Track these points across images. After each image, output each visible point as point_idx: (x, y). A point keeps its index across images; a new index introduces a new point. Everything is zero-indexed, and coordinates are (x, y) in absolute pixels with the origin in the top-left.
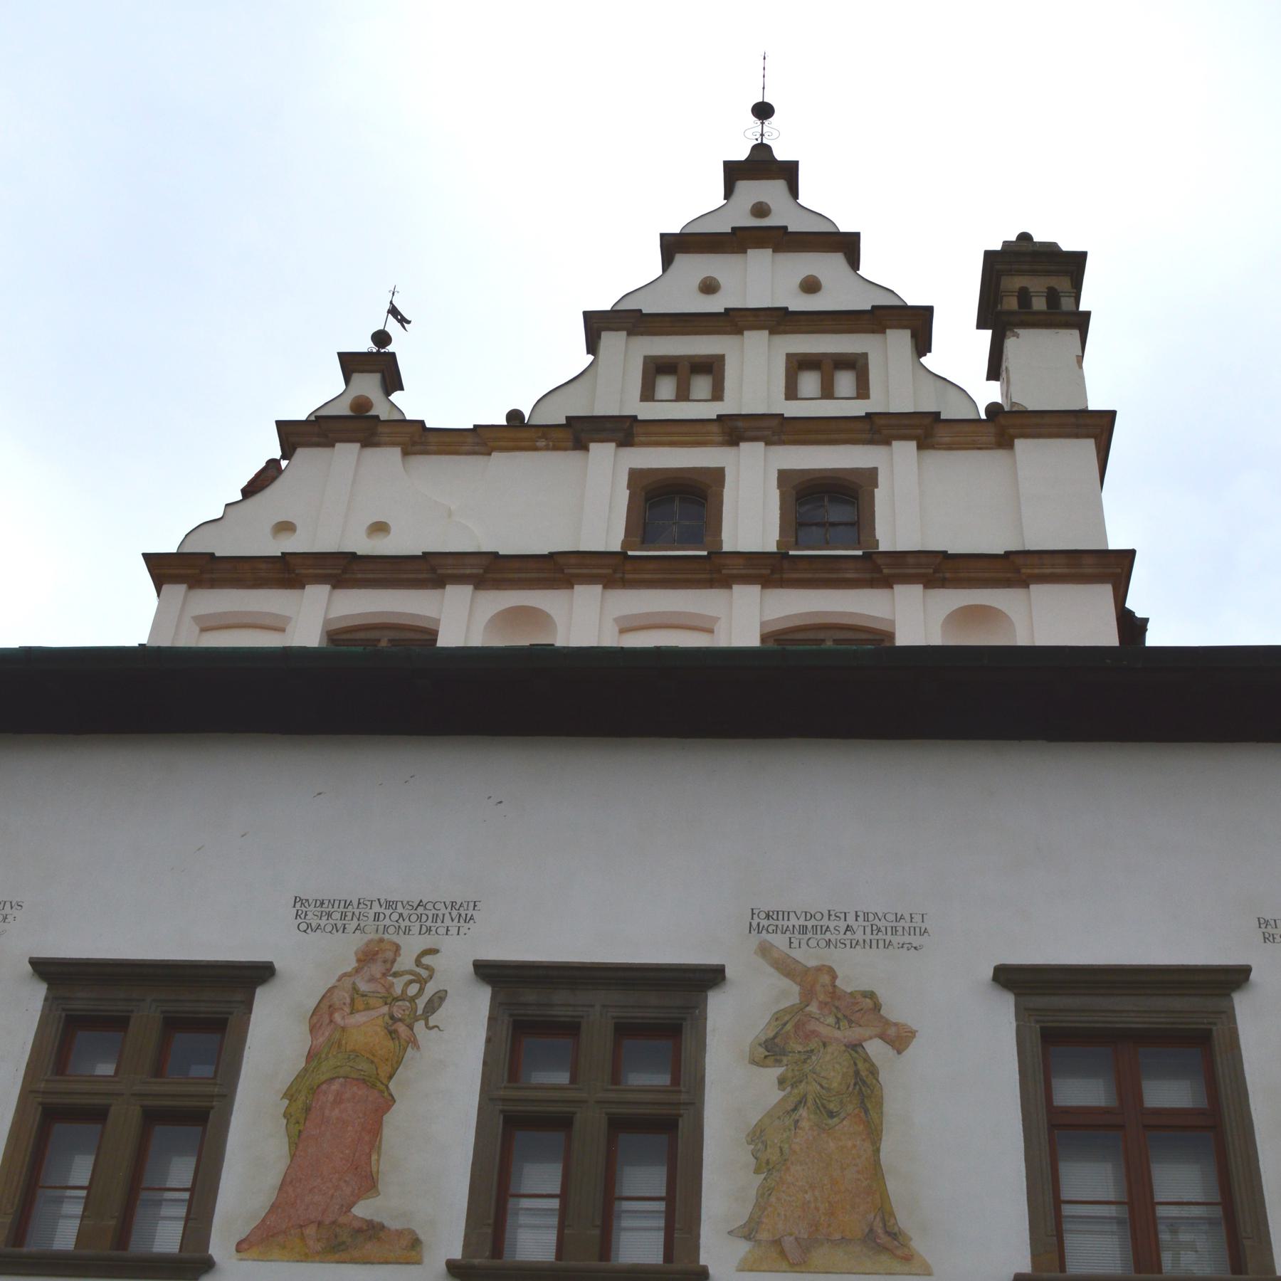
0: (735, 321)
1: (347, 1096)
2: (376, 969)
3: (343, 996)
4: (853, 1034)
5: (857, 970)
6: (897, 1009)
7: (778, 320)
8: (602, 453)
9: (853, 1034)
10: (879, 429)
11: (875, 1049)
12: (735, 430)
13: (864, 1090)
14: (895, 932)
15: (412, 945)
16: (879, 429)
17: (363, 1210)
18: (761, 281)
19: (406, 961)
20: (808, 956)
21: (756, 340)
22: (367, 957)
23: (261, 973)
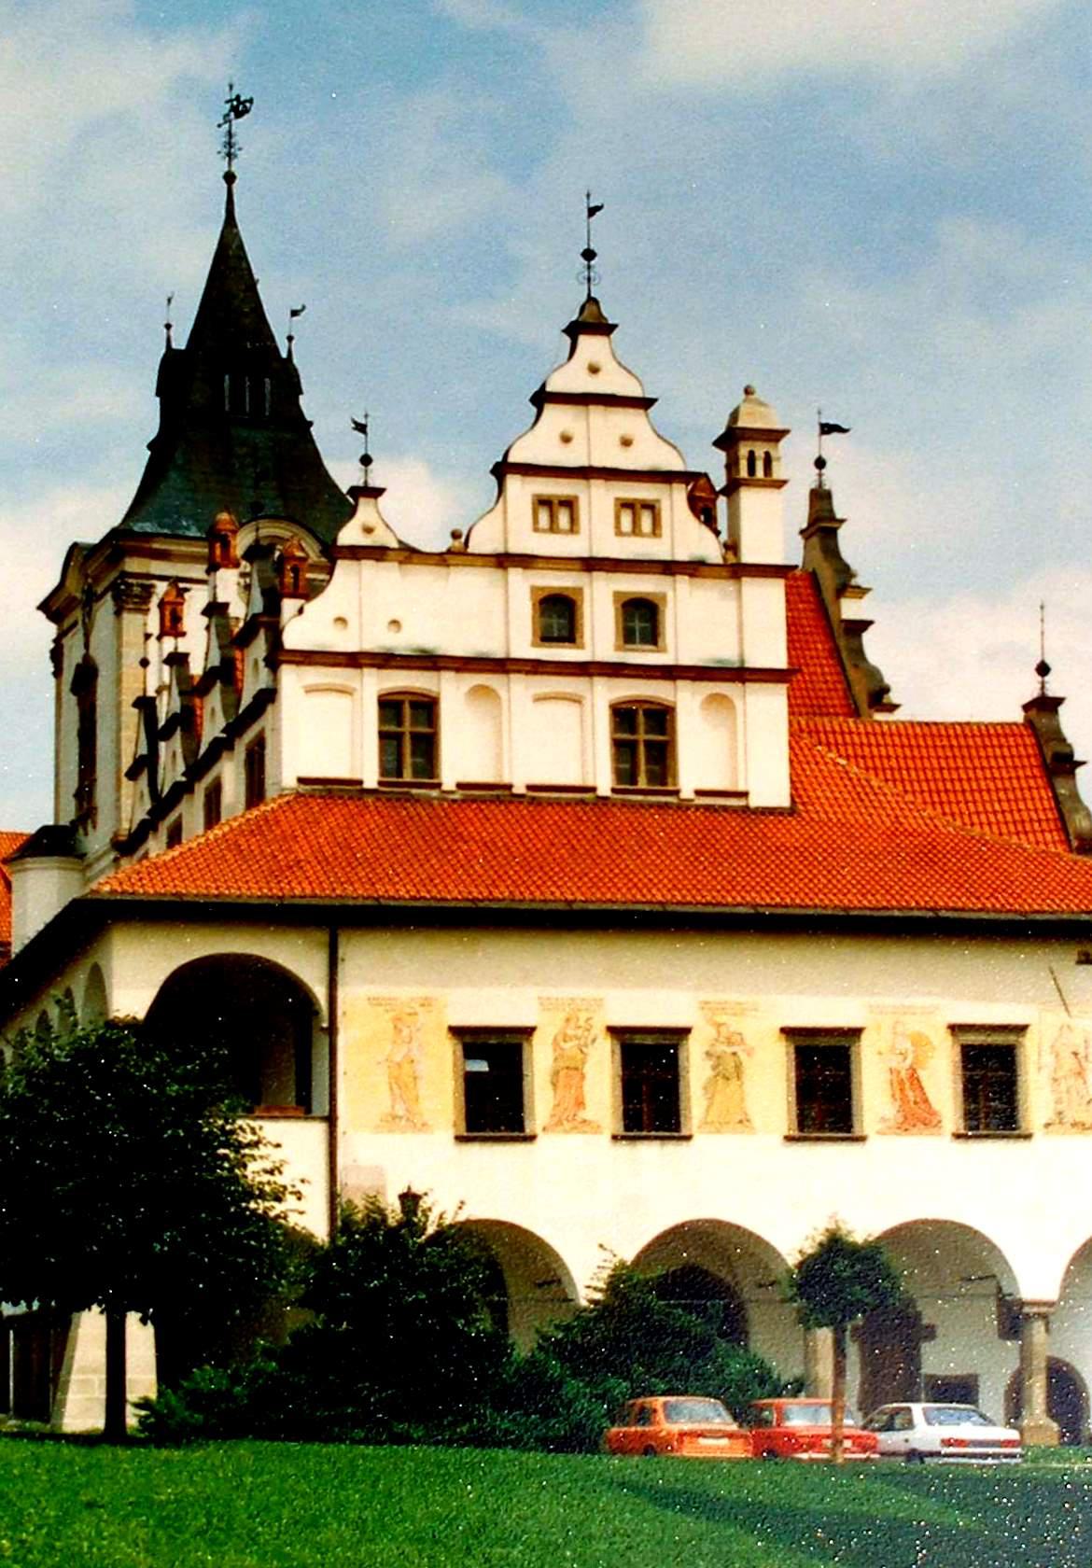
1: (570, 1073)
2: (572, 1024)
3: (560, 1038)
4: (735, 1049)
5: (735, 1024)
6: (750, 1041)
8: (515, 574)
9: (735, 1049)
10: (669, 568)
11: (743, 1056)
12: (591, 564)
13: (738, 1067)
16: (669, 568)
18: (598, 437)
19: (582, 1023)
20: (721, 1019)
22: (568, 1020)
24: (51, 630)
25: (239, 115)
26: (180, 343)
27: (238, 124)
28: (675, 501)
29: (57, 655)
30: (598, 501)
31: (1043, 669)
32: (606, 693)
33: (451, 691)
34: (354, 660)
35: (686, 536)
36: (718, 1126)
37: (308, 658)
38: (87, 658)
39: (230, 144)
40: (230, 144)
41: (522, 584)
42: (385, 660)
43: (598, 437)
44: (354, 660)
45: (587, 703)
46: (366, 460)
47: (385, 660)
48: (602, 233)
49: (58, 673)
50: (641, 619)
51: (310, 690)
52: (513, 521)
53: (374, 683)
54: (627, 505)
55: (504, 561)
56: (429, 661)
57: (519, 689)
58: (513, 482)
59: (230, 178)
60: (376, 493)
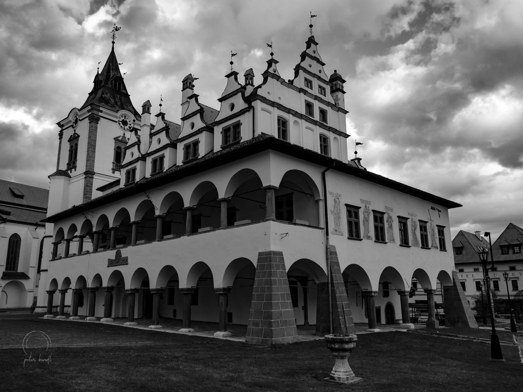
0: (314, 75)
5: (391, 214)
7: (319, 78)
8: (302, 94)
10: (328, 104)
12: (316, 98)
14: (392, 210)
15: (368, 206)
17: (369, 235)
18: (315, 68)
20: (388, 212)
21: (316, 79)
23: (360, 208)
24: (60, 129)
25: (116, 30)
26: (100, 73)
27: (116, 32)
28: (328, 88)
29: (61, 135)
30: (316, 83)
31: (356, 153)
32: (319, 130)
33: (291, 119)
34: (273, 104)
35: (329, 98)
36: (390, 241)
37: (264, 100)
38: (75, 134)
39: (114, 36)
40: (114, 36)
41: (303, 98)
42: (280, 107)
43: (315, 68)
44: (273, 104)
45: (315, 131)
46: (272, 54)
47: (280, 107)
48: (314, 21)
49: (61, 138)
50: (323, 113)
51: (263, 110)
52: (300, 83)
53: (277, 112)
54: (320, 87)
55: (301, 90)
56: (289, 111)
57: (303, 123)
58: (301, 72)
59: (113, 43)
60: (277, 62)
